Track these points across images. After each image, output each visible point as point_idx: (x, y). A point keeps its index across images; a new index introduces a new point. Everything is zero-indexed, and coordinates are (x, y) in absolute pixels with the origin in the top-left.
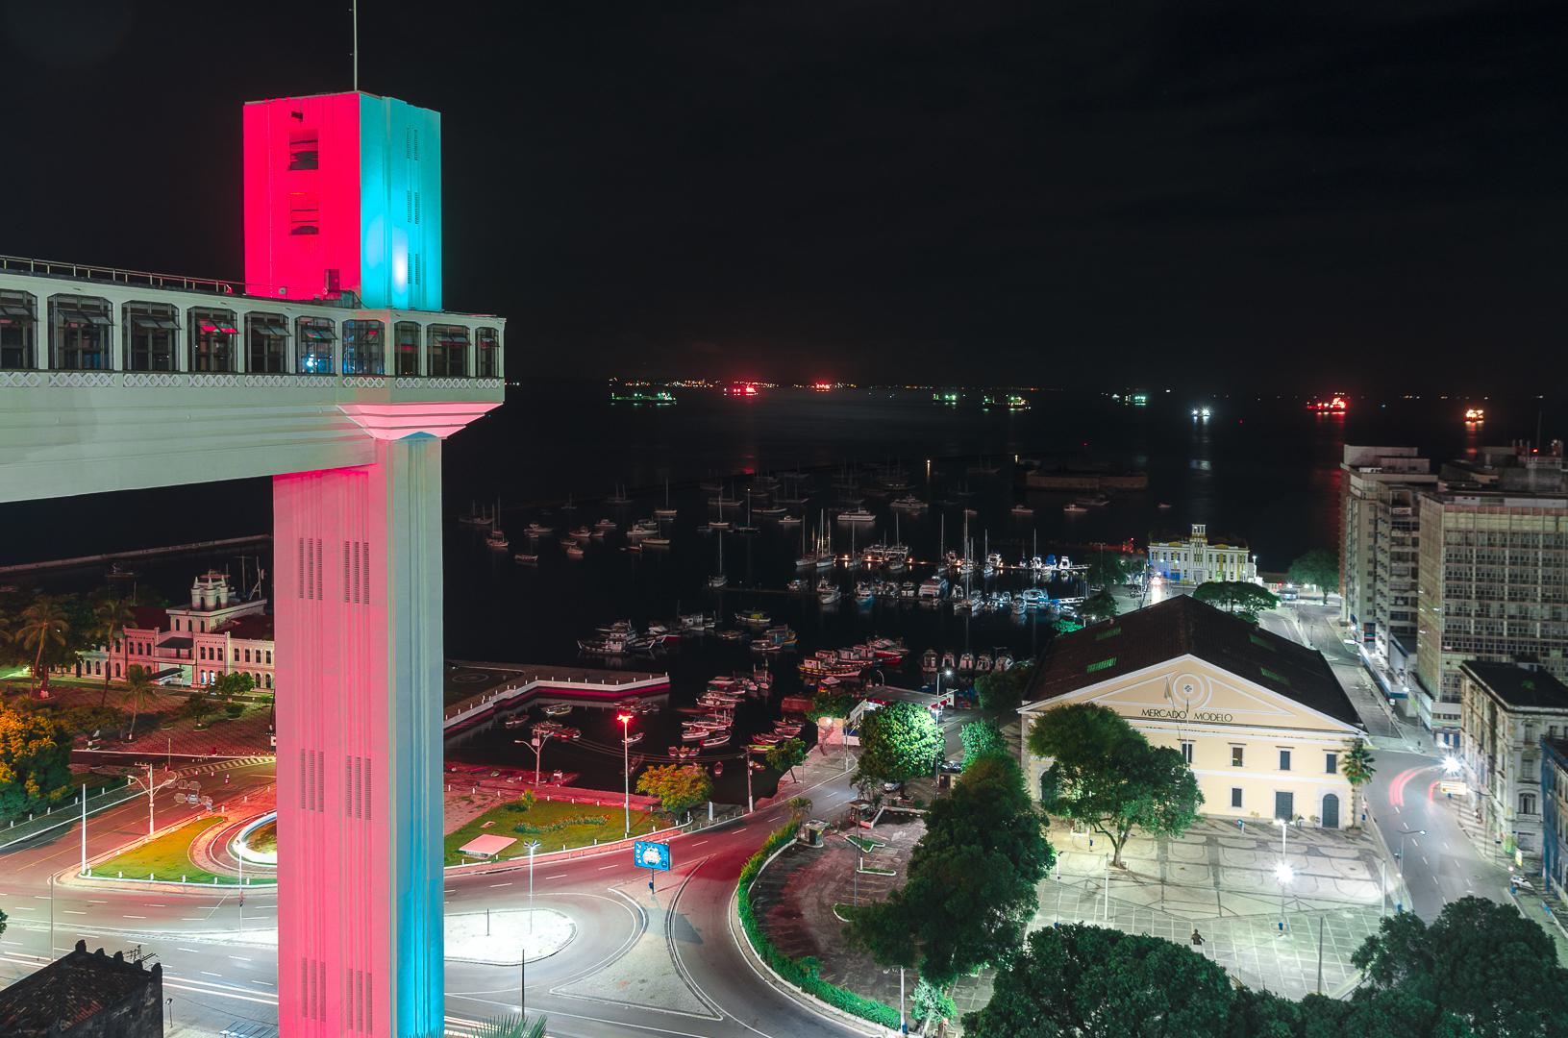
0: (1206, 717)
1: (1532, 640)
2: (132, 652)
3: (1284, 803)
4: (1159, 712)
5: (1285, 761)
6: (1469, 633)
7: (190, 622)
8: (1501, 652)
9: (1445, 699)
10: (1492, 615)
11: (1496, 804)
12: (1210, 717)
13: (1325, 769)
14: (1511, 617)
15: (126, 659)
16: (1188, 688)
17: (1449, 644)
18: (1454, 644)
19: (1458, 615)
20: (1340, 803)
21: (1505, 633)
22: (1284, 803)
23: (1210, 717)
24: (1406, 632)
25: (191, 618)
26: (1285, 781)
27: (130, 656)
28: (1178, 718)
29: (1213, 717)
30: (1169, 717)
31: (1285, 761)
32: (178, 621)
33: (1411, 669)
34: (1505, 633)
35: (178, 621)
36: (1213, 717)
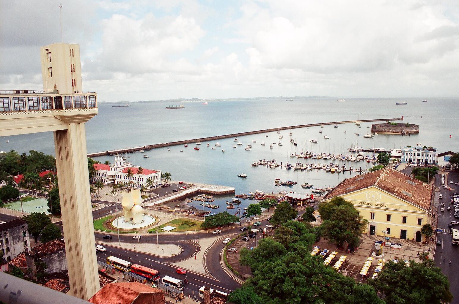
0: (379, 205)
2: (102, 176)
3: (403, 233)
5: (404, 220)
7: (117, 169)
12: (380, 205)
15: (101, 178)
22: (403, 233)
23: (380, 205)
25: (115, 168)
26: (404, 227)
27: (102, 177)
29: (381, 205)
31: (404, 220)
32: (112, 168)
35: (112, 168)
36: (381, 205)
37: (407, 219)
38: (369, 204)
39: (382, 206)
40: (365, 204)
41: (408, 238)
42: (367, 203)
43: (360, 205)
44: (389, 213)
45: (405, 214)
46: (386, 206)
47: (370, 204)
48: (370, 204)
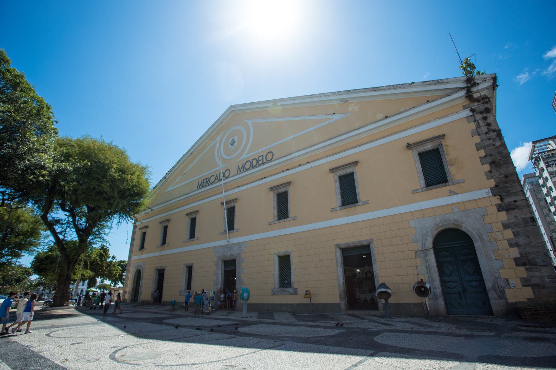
4: (209, 180)
12: (251, 164)
20: (477, 245)
23: (251, 164)
36: (255, 163)
39: (258, 161)
40: (212, 180)
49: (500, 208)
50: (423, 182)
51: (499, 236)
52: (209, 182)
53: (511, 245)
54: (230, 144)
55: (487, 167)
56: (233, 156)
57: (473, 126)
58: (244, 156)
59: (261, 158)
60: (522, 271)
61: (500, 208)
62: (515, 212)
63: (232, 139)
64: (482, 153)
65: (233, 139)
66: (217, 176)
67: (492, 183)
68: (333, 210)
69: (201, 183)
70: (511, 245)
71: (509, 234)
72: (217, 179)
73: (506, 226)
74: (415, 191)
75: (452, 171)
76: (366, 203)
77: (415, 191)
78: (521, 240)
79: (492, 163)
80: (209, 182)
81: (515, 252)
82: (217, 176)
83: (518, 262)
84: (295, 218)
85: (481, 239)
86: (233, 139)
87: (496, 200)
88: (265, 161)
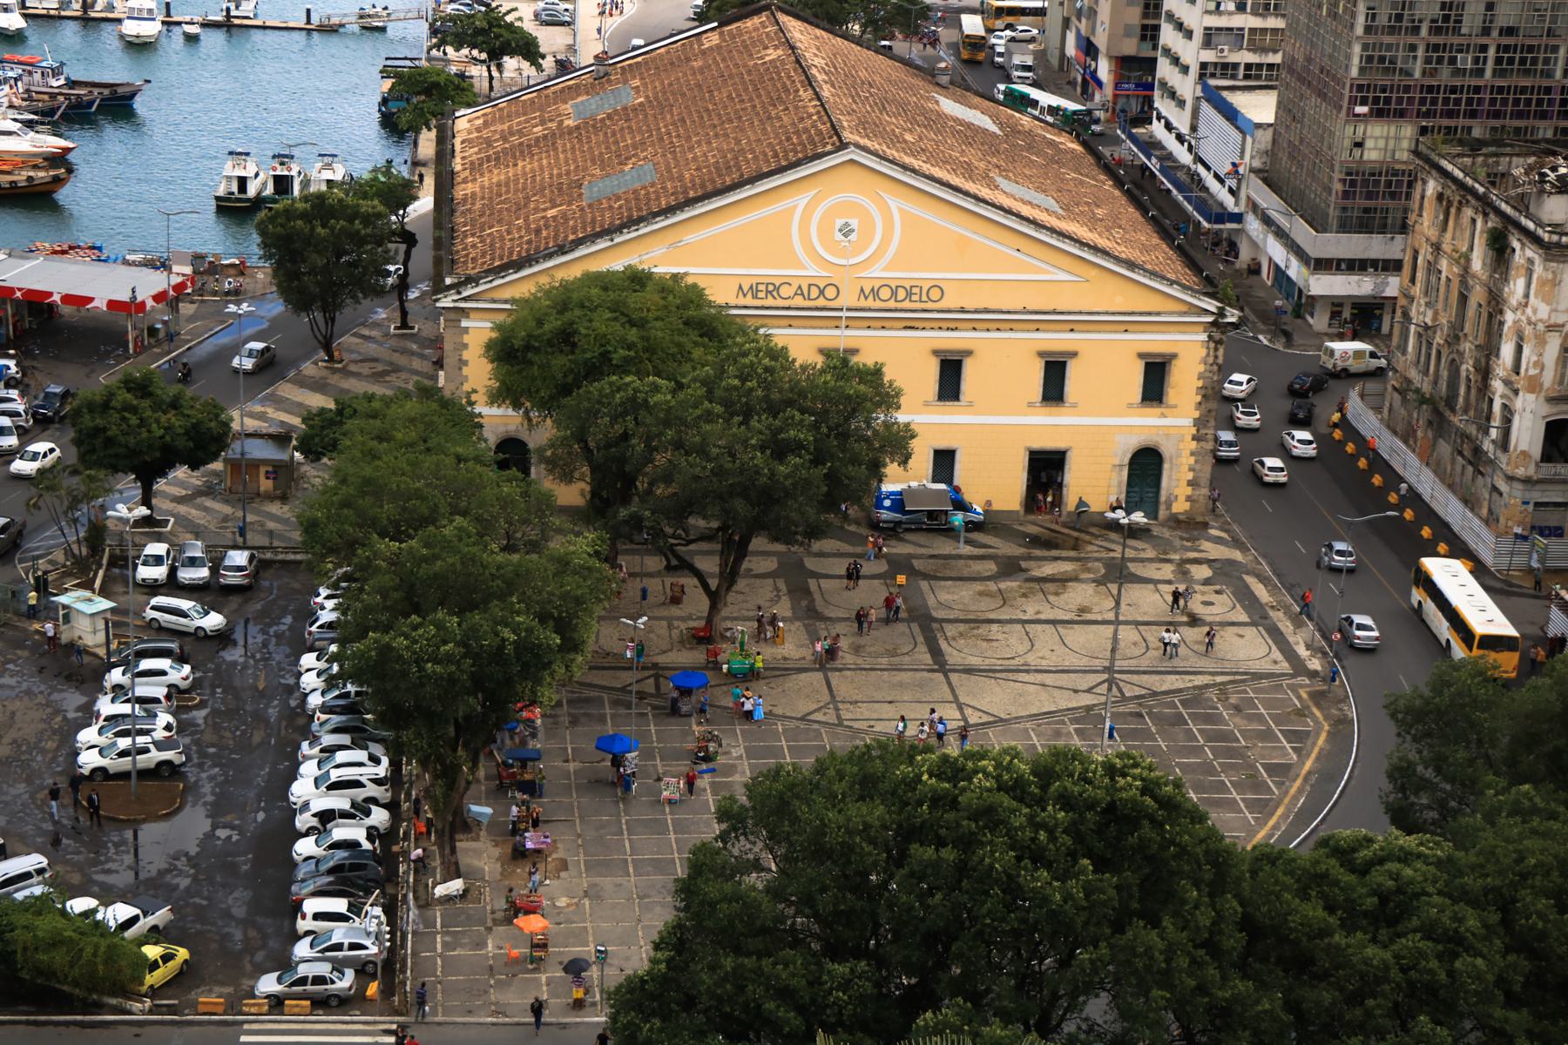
0: (886, 293)
1: (1545, 83)
4: (777, 289)
6: (1409, 74)
8: (1473, 114)
9: (1345, 227)
10: (1463, 31)
11: (1487, 446)
12: (894, 293)
13: (1139, 397)
14: (1510, 31)
16: (846, 231)
17: (1364, 102)
18: (1376, 100)
19: (1392, 30)
20: (1166, 466)
21: (1488, 73)
23: (894, 293)
24: (1234, 77)
28: (821, 302)
29: (901, 294)
30: (799, 301)
33: (1257, 164)
34: (1488, 73)
36: (901, 294)
37: (1073, 372)
38: (815, 292)
39: (909, 294)
40: (785, 291)
41: (1081, 503)
42: (795, 287)
43: (749, 301)
44: (952, 340)
45: (1057, 340)
46: (935, 294)
47: (822, 292)
48: (822, 292)
49: (1194, 438)
50: (1140, 397)
51: (1184, 460)
52: (775, 293)
53: (1190, 470)
54: (840, 230)
55: (1199, 398)
56: (852, 261)
57: (1204, 352)
58: (877, 272)
59: (914, 291)
60: (1189, 491)
61: (1194, 438)
62: (1203, 444)
63: (843, 221)
64: (1200, 383)
65: (847, 224)
66: (800, 287)
67: (1197, 414)
68: (1030, 405)
69: (751, 287)
70: (1190, 470)
71: (1192, 460)
72: (802, 294)
73: (1192, 454)
74: (1130, 406)
75: (1171, 395)
76: (1074, 405)
77: (1130, 406)
78: (1198, 467)
79: (1204, 396)
80: (775, 293)
81: (1190, 476)
82: (800, 287)
83: (1190, 483)
84: (970, 404)
85: (1171, 463)
86: (847, 224)
87: (1194, 431)
88: (924, 298)
